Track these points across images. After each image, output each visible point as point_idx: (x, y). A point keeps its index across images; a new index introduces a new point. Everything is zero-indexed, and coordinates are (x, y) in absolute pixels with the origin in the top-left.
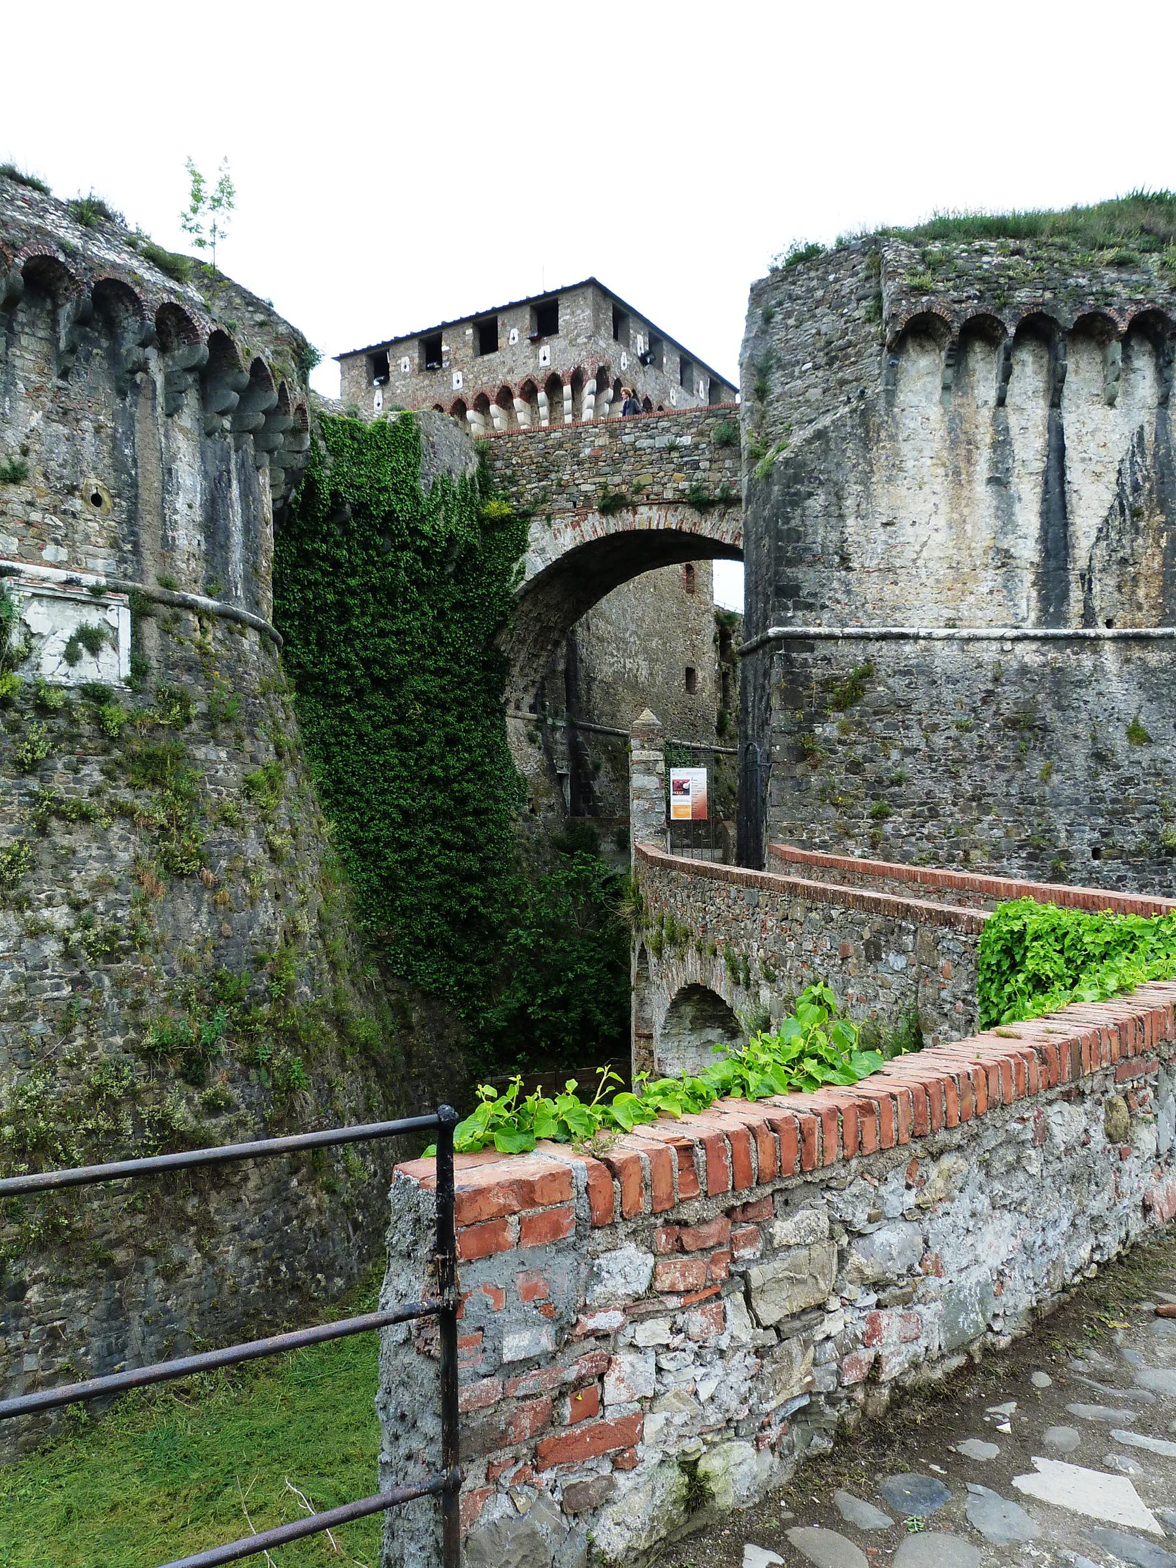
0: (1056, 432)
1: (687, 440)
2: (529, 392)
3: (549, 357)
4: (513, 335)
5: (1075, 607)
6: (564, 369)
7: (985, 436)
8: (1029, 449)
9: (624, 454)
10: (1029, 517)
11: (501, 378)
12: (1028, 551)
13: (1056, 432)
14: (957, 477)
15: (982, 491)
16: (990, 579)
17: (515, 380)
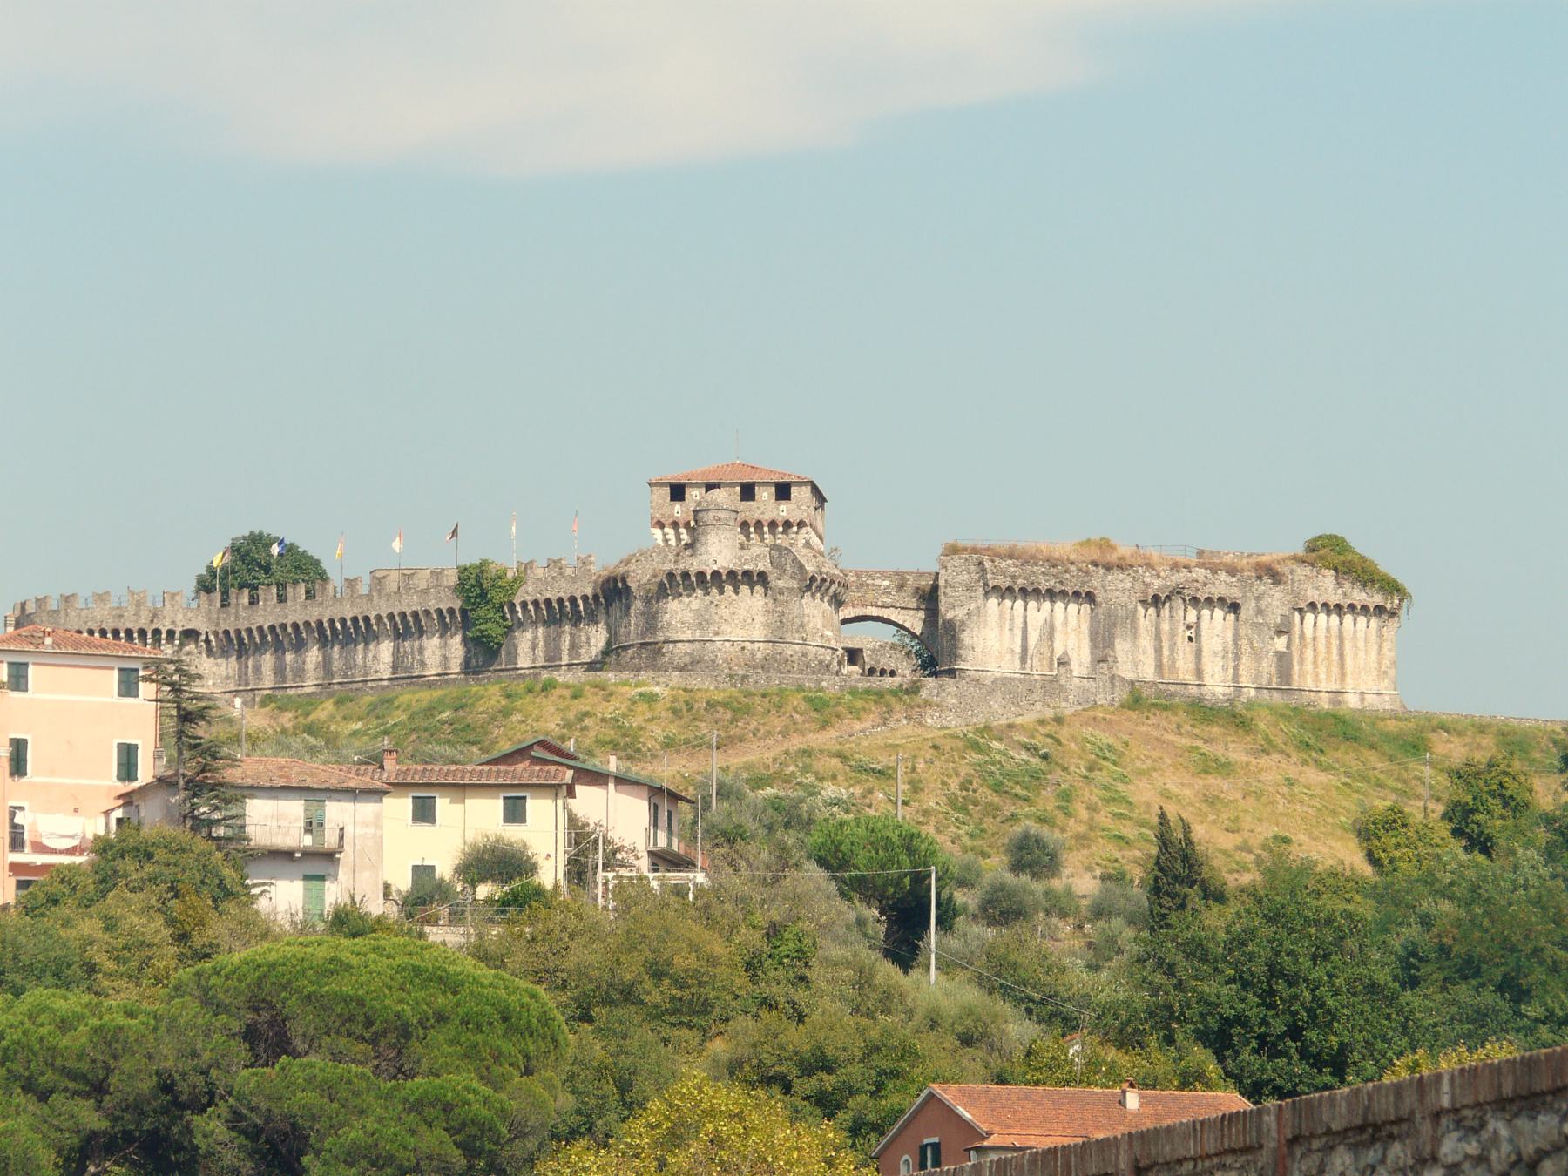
0: (1025, 617)
1: (886, 583)
2: (773, 525)
3: (784, 510)
4: (765, 495)
5: (1028, 665)
6: (794, 519)
7: (1008, 617)
8: (1019, 622)
9: (862, 585)
10: (1018, 641)
11: (757, 516)
12: (1018, 650)
13: (1025, 617)
14: (1001, 628)
15: (1007, 631)
16: (1008, 657)
17: (766, 518)
